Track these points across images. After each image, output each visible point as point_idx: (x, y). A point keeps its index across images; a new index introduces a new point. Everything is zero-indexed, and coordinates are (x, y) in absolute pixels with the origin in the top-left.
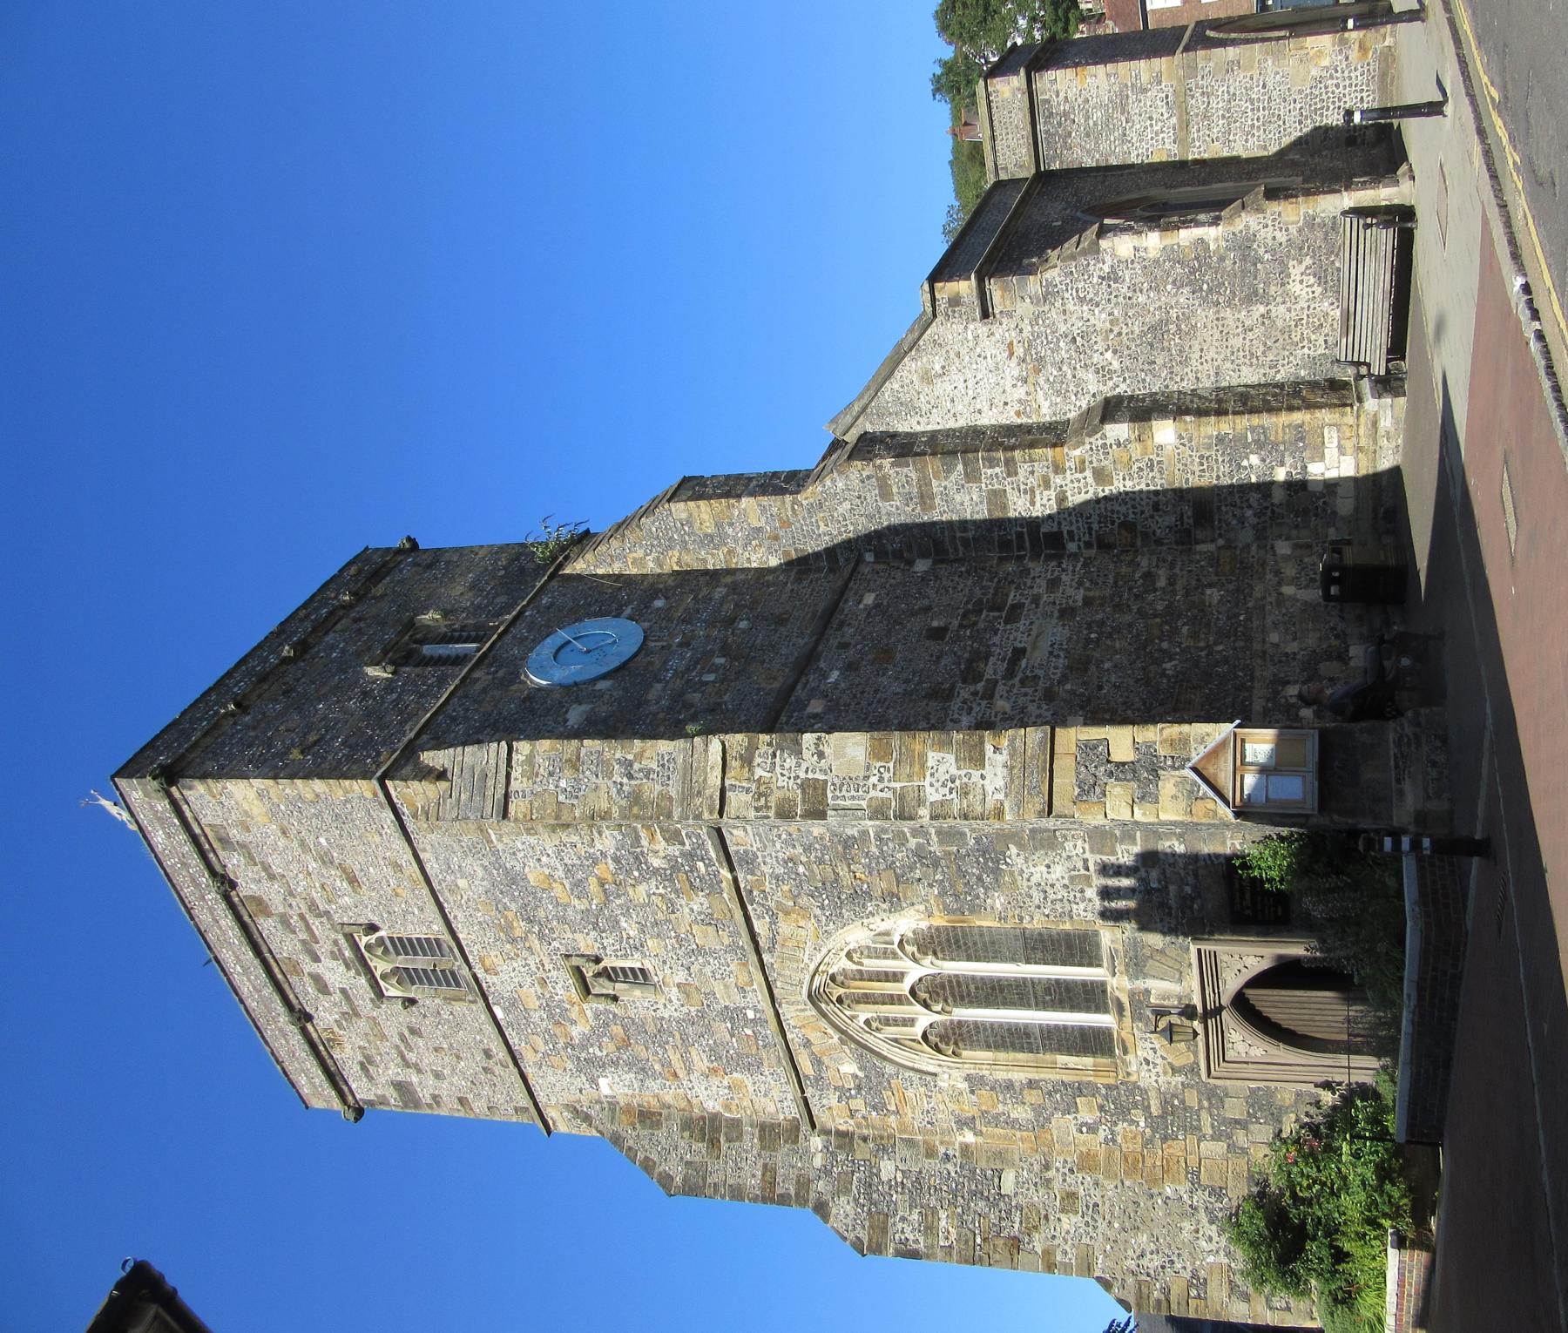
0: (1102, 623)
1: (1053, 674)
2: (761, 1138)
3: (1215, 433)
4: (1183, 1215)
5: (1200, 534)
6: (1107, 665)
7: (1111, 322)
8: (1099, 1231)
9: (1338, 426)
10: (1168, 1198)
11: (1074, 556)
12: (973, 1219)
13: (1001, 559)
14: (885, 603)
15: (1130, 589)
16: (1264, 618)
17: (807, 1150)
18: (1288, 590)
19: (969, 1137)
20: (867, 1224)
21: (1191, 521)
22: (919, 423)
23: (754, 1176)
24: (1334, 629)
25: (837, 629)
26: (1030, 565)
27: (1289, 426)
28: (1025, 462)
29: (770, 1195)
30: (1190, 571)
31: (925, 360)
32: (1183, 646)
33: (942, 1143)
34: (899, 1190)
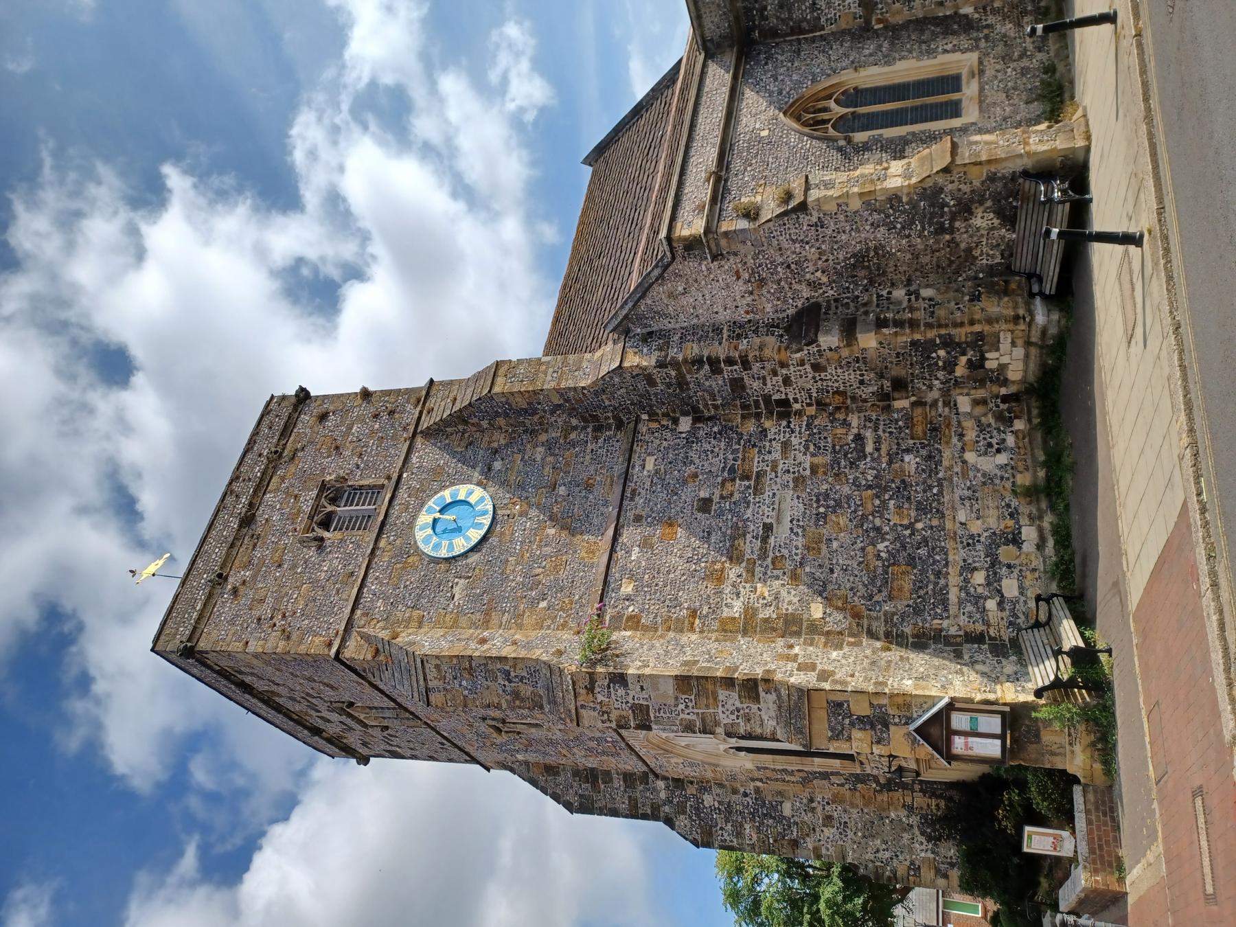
0: (827, 496)
1: (796, 555)
2: (625, 781)
3: (909, 340)
5: (896, 395)
6: (835, 544)
7: (820, 254)
8: (849, 837)
9: (1012, 332)
10: (893, 819)
11: (799, 413)
12: (767, 830)
13: (743, 417)
14: (663, 470)
15: (845, 455)
16: (953, 492)
17: (654, 789)
18: (970, 457)
19: (759, 784)
20: (699, 831)
21: (890, 389)
22: (670, 322)
23: (624, 803)
24: (1008, 506)
26: (767, 424)
27: (971, 333)
28: (757, 362)
29: (634, 813)
30: (891, 433)
31: (669, 285)
32: (891, 523)
33: (742, 786)
34: (717, 811)
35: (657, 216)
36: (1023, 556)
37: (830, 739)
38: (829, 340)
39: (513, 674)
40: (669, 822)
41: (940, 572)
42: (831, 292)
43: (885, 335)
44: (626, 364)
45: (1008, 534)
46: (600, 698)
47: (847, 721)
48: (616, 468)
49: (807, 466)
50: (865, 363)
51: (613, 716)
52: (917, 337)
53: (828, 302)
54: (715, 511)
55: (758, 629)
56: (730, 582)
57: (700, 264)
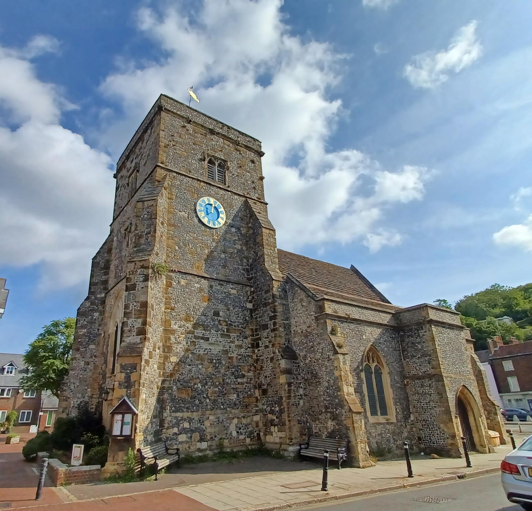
0: (220, 363)
1: (196, 351)
4: (82, 394)
5: (260, 391)
6: (200, 367)
7: (317, 359)
9: (286, 437)
11: (254, 352)
13: (252, 329)
15: (237, 371)
18: (235, 421)
19: (103, 335)
24: (215, 437)
25: (219, 284)
26: (249, 339)
29: (91, 284)
30: (245, 389)
32: (209, 389)
35: (332, 295)
36: (195, 443)
37: (121, 365)
38: (283, 364)
39: (149, 235)
40: (87, 299)
41: (189, 409)
42: (302, 364)
43: (285, 386)
44: (274, 282)
45: (204, 437)
46: (139, 271)
47: (129, 371)
48: (232, 278)
49: (232, 355)
50: (274, 378)
51: (131, 276)
52: (284, 399)
53: (298, 363)
54: (214, 318)
55: (166, 335)
56: (185, 324)
57: (314, 312)
